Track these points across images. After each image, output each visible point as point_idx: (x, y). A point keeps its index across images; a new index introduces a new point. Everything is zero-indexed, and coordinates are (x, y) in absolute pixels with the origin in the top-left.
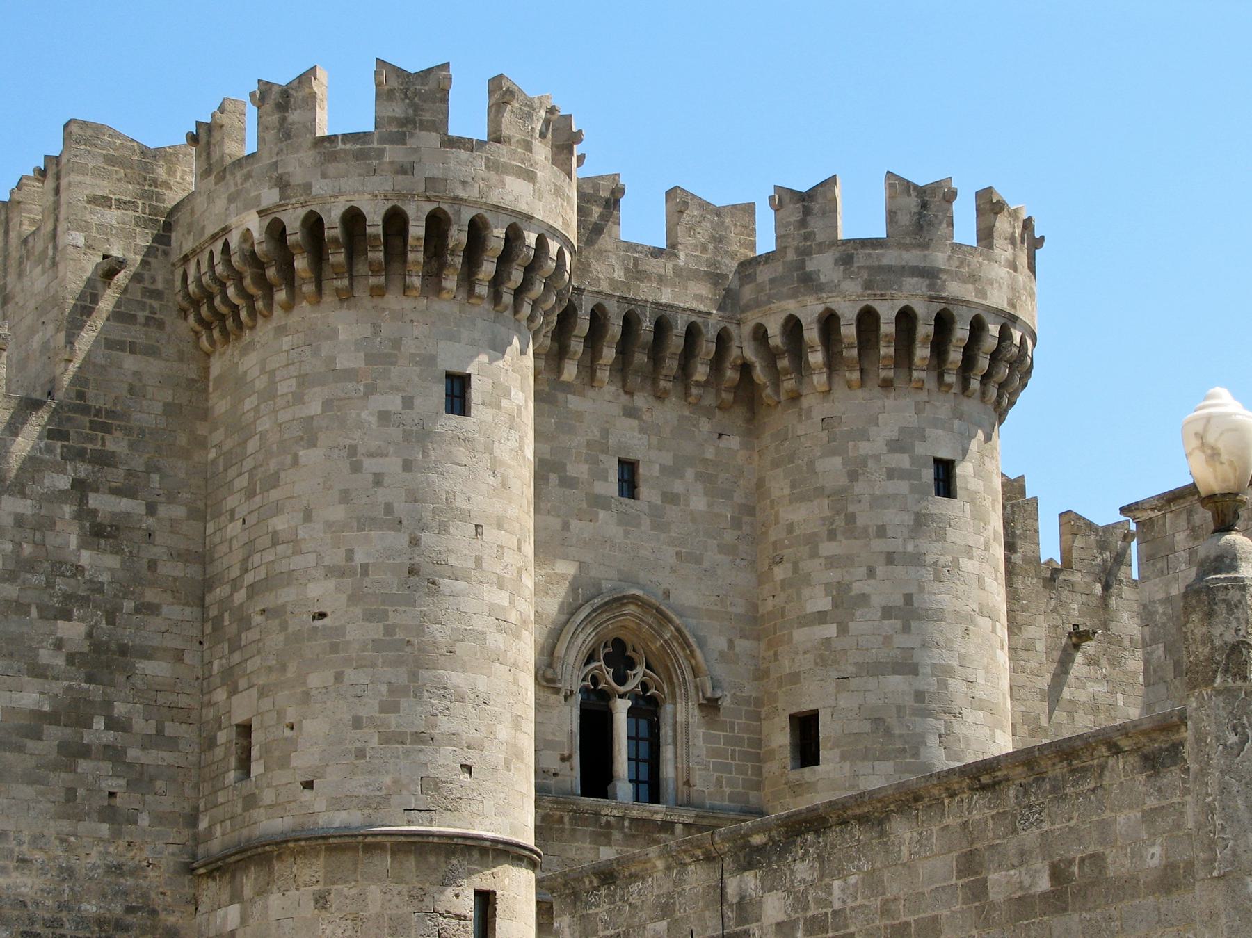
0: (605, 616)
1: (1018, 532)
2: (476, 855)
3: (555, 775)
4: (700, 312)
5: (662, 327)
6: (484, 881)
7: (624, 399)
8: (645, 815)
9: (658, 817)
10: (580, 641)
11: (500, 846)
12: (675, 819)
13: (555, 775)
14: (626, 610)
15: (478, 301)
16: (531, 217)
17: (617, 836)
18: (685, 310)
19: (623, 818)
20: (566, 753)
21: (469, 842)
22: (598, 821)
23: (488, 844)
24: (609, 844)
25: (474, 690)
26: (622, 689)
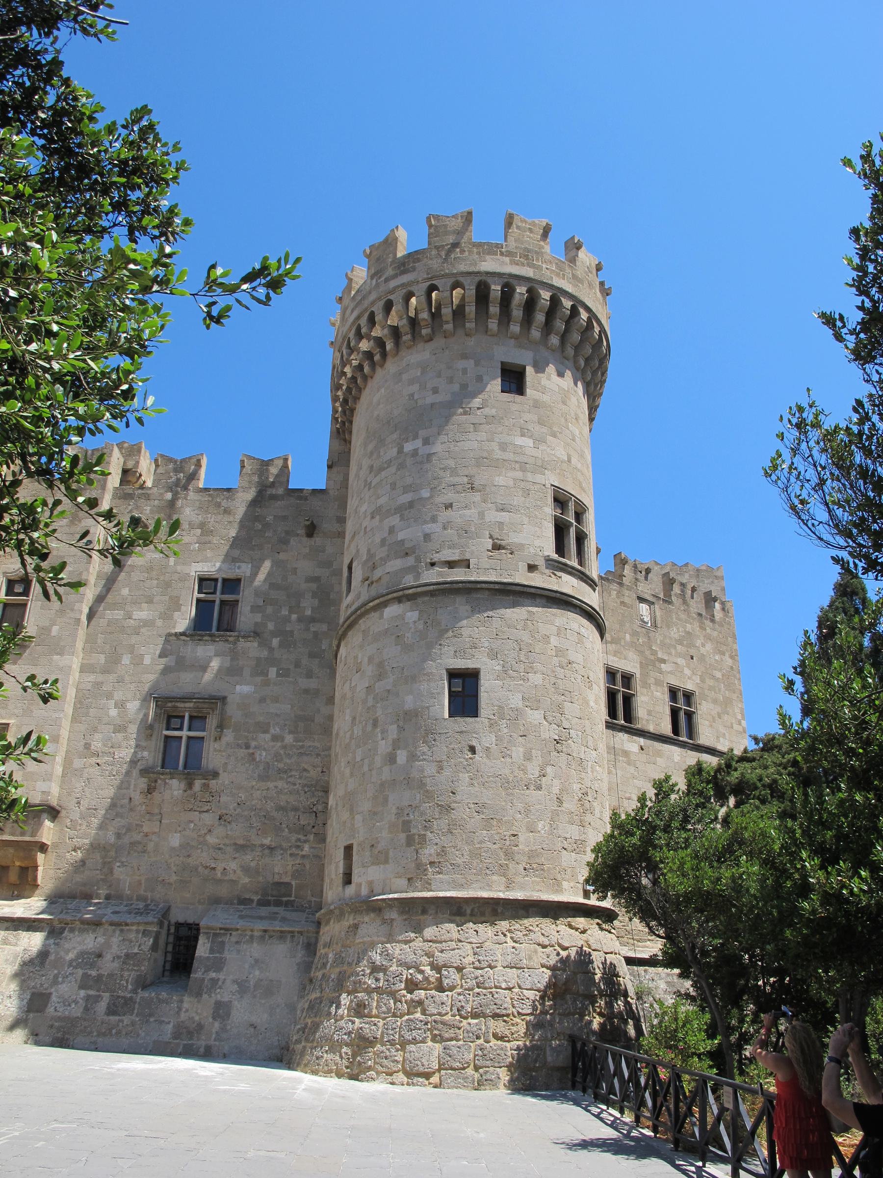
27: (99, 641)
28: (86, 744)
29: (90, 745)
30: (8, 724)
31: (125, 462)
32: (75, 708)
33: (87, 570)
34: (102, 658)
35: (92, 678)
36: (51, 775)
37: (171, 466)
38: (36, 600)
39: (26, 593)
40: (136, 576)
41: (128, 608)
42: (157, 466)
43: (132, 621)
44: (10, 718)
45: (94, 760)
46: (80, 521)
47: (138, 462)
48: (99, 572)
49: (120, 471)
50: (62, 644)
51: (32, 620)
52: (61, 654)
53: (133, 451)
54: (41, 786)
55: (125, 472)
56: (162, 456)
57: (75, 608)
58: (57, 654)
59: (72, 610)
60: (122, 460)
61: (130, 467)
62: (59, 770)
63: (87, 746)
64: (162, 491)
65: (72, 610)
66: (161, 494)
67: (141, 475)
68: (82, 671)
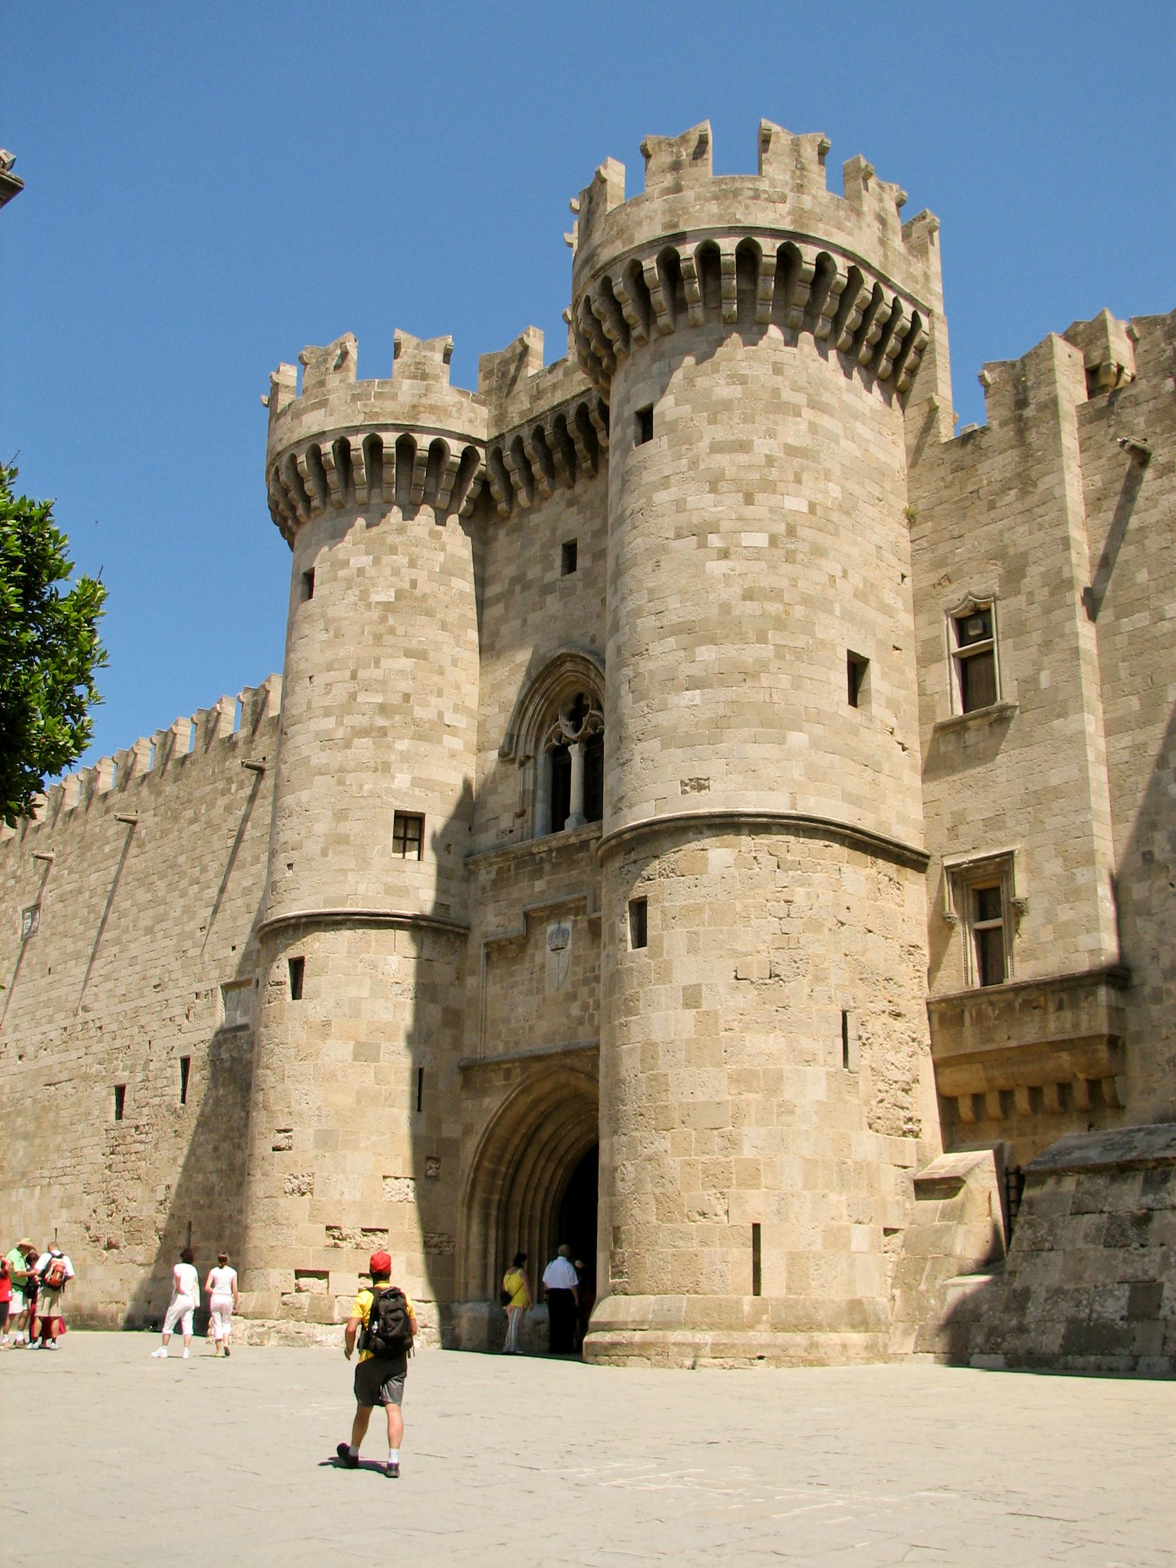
0: (549, 681)
1: (1029, 384)
2: (291, 932)
3: (511, 831)
4: (584, 392)
5: (560, 422)
6: (294, 952)
7: (568, 494)
8: (562, 842)
9: (573, 840)
10: (530, 712)
11: (304, 920)
12: (584, 837)
13: (511, 831)
14: (563, 670)
15: (318, 512)
16: (324, 432)
17: (547, 867)
18: (573, 398)
19: (550, 850)
20: (518, 810)
21: (282, 924)
22: (534, 860)
23: (293, 921)
24: (541, 877)
25: (299, 804)
26: (573, 736)
27: (1122, 674)
28: (1144, 854)
29: (1150, 853)
30: (1011, 853)
31: (1086, 358)
32: (1113, 800)
33: (1068, 561)
34: (1134, 703)
35: (1126, 740)
36: (1097, 920)
37: (1159, 333)
38: (1004, 639)
39: (987, 633)
40: (1153, 543)
41: (1154, 602)
42: (1135, 341)
43: (1166, 624)
44: (1013, 842)
45: (1162, 882)
46: (1035, 485)
47: (1107, 348)
48: (1092, 558)
49: (1081, 376)
50: (1061, 697)
51: (1006, 672)
52: (1062, 715)
53: (1088, 336)
54: (1085, 941)
55: (1093, 373)
56: (1138, 321)
57: (1067, 631)
58: (1059, 716)
59: (1062, 636)
60: (1079, 356)
61: (1096, 362)
62: (1108, 909)
63: (1148, 857)
64: (1154, 382)
65: (1062, 636)
66: (1155, 387)
67: (1120, 369)
68: (1108, 733)
